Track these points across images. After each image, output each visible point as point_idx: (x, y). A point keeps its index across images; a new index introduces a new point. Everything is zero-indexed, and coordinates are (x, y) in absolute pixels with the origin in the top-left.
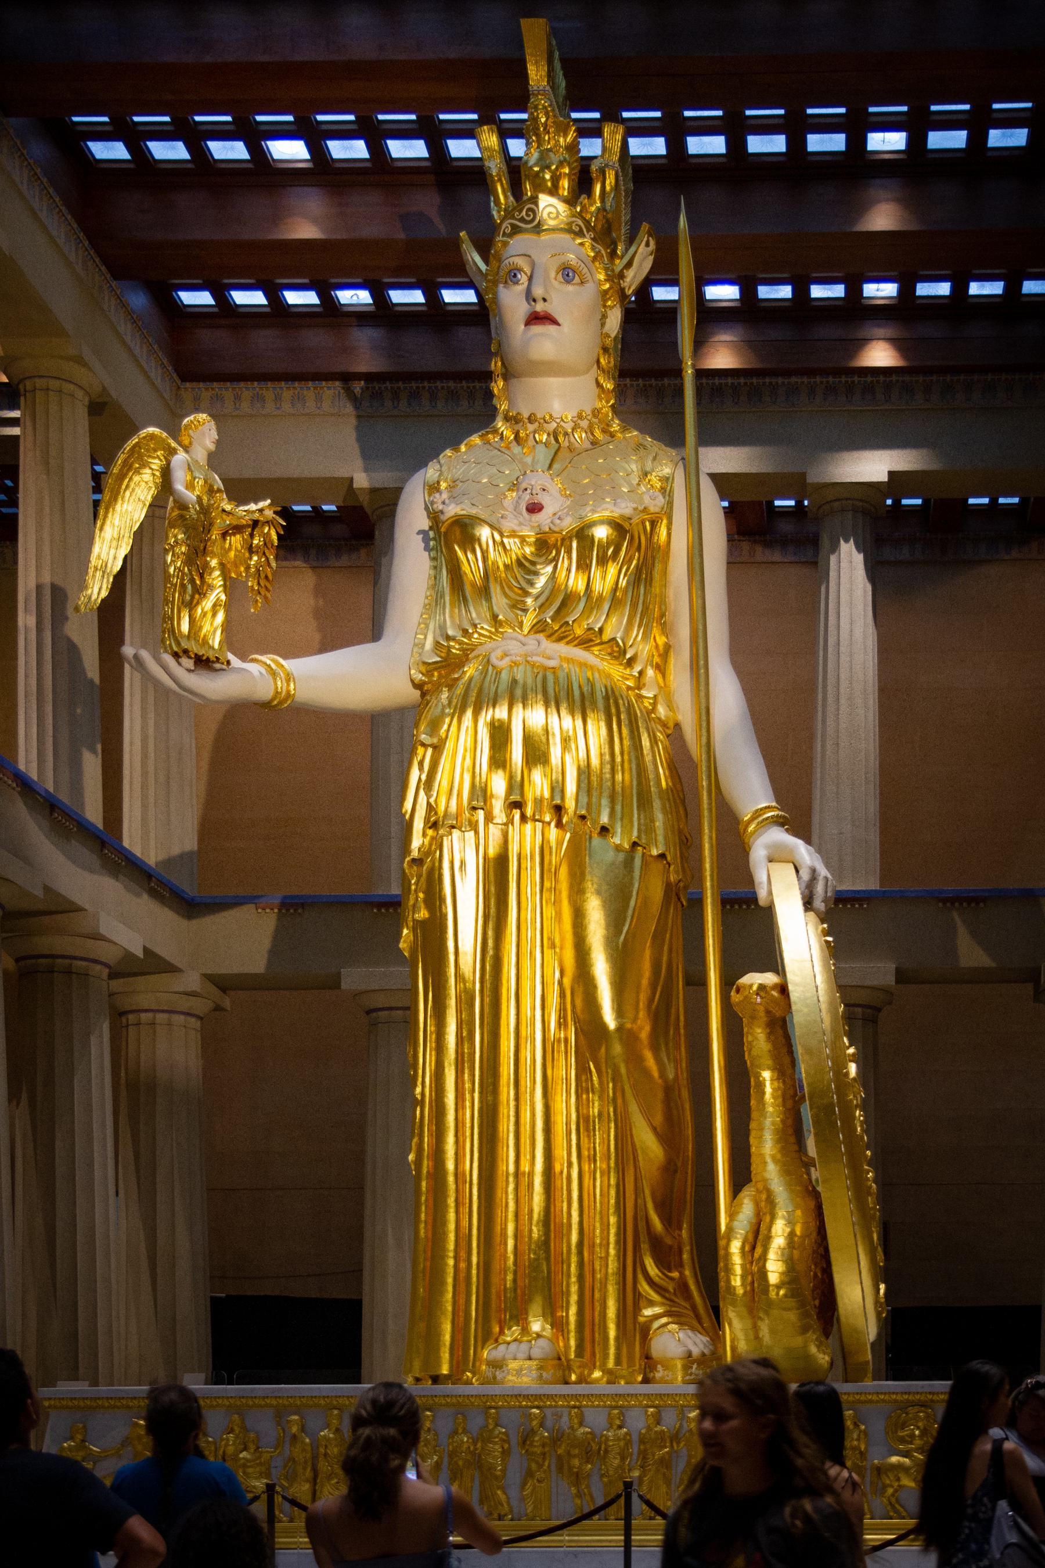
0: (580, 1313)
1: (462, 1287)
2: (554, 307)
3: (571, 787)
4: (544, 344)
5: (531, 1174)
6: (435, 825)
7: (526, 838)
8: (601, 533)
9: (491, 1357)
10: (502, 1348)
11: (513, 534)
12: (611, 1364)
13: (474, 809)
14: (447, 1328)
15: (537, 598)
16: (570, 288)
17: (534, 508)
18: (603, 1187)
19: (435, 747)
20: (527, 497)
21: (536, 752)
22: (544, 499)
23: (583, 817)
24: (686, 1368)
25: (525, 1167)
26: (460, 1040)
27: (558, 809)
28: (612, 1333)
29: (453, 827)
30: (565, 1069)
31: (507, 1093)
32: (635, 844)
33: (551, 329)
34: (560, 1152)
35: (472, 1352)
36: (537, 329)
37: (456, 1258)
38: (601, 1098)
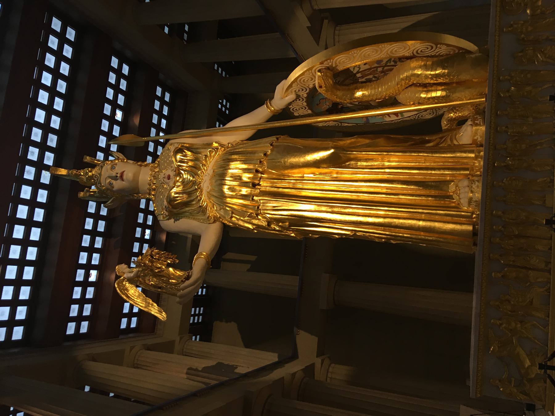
0: (448, 169)
1: (433, 217)
2: (119, 172)
3: (251, 167)
4: (129, 175)
5: (387, 188)
6: (257, 215)
7: (265, 185)
8: (179, 157)
9: (466, 204)
10: (462, 201)
11: (175, 183)
12: (473, 155)
13: (253, 199)
14: (450, 226)
15: (193, 177)
16: (116, 168)
17: (169, 177)
18: (394, 160)
19: (233, 213)
20: (166, 180)
21: (237, 178)
22: (167, 174)
23: (261, 162)
24: (477, 125)
25: (384, 191)
26: (332, 212)
27: (257, 171)
28: (458, 155)
29: (258, 208)
30: (346, 173)
31: (354, 196)
32: (271, 145)
33: (125, 173)
34: (380, 177)
35: (463, 213)
36: (124, 177)
37: (419, 220)
38: (360, 160)
